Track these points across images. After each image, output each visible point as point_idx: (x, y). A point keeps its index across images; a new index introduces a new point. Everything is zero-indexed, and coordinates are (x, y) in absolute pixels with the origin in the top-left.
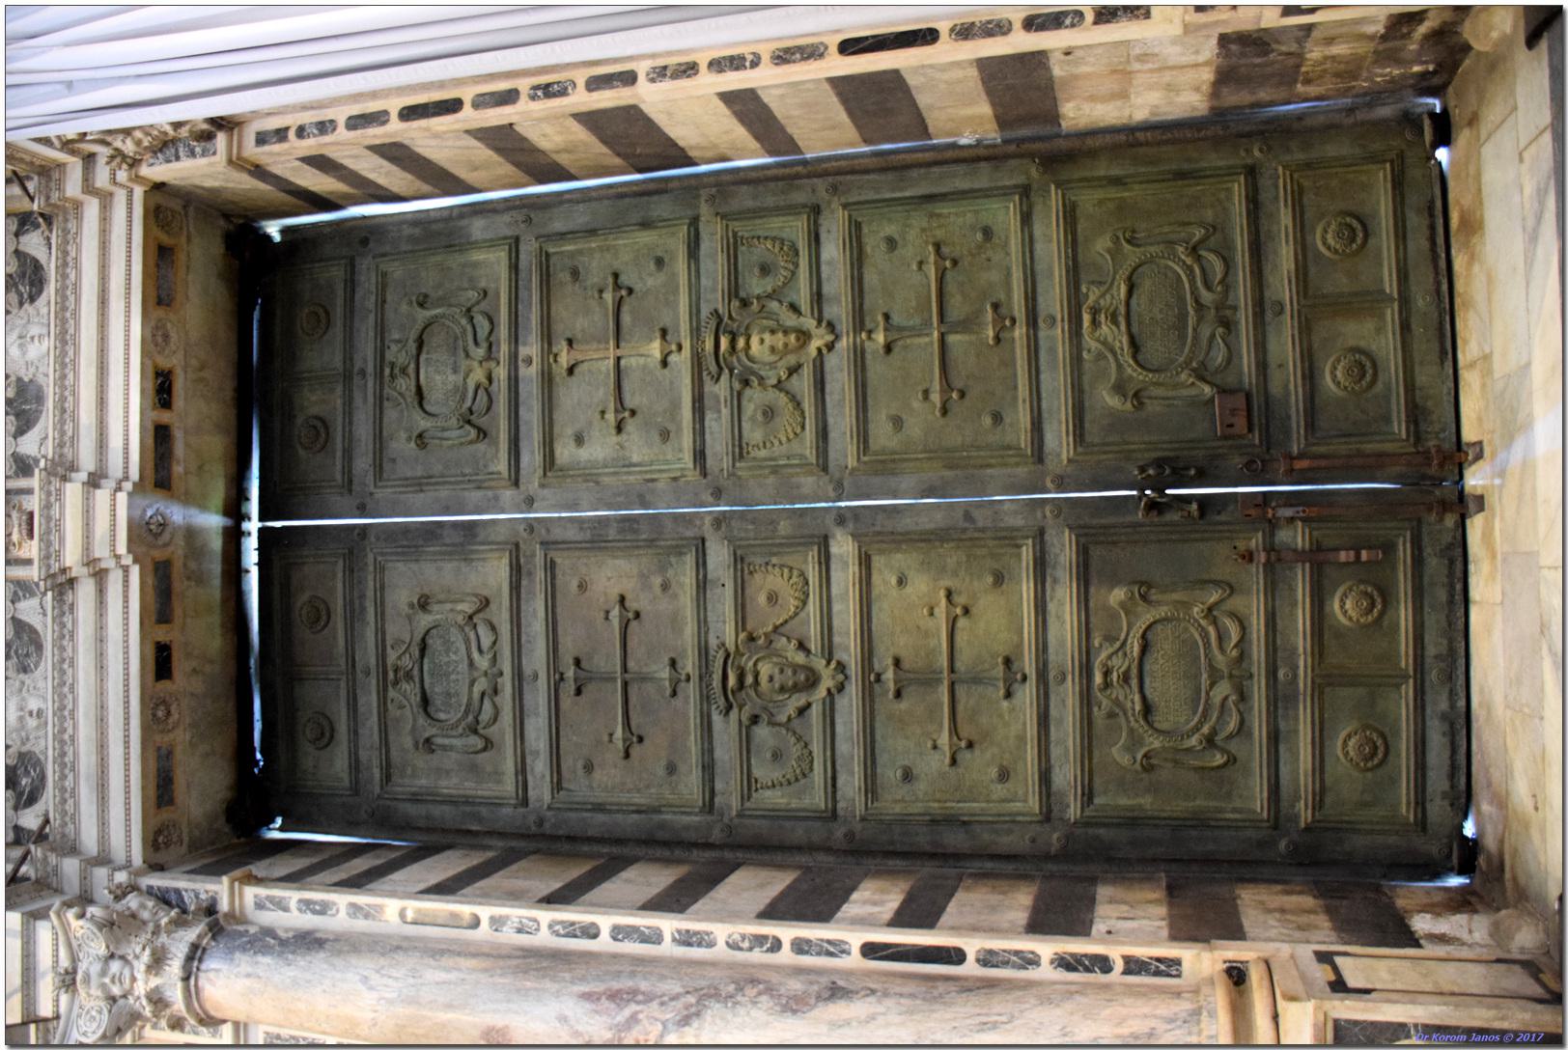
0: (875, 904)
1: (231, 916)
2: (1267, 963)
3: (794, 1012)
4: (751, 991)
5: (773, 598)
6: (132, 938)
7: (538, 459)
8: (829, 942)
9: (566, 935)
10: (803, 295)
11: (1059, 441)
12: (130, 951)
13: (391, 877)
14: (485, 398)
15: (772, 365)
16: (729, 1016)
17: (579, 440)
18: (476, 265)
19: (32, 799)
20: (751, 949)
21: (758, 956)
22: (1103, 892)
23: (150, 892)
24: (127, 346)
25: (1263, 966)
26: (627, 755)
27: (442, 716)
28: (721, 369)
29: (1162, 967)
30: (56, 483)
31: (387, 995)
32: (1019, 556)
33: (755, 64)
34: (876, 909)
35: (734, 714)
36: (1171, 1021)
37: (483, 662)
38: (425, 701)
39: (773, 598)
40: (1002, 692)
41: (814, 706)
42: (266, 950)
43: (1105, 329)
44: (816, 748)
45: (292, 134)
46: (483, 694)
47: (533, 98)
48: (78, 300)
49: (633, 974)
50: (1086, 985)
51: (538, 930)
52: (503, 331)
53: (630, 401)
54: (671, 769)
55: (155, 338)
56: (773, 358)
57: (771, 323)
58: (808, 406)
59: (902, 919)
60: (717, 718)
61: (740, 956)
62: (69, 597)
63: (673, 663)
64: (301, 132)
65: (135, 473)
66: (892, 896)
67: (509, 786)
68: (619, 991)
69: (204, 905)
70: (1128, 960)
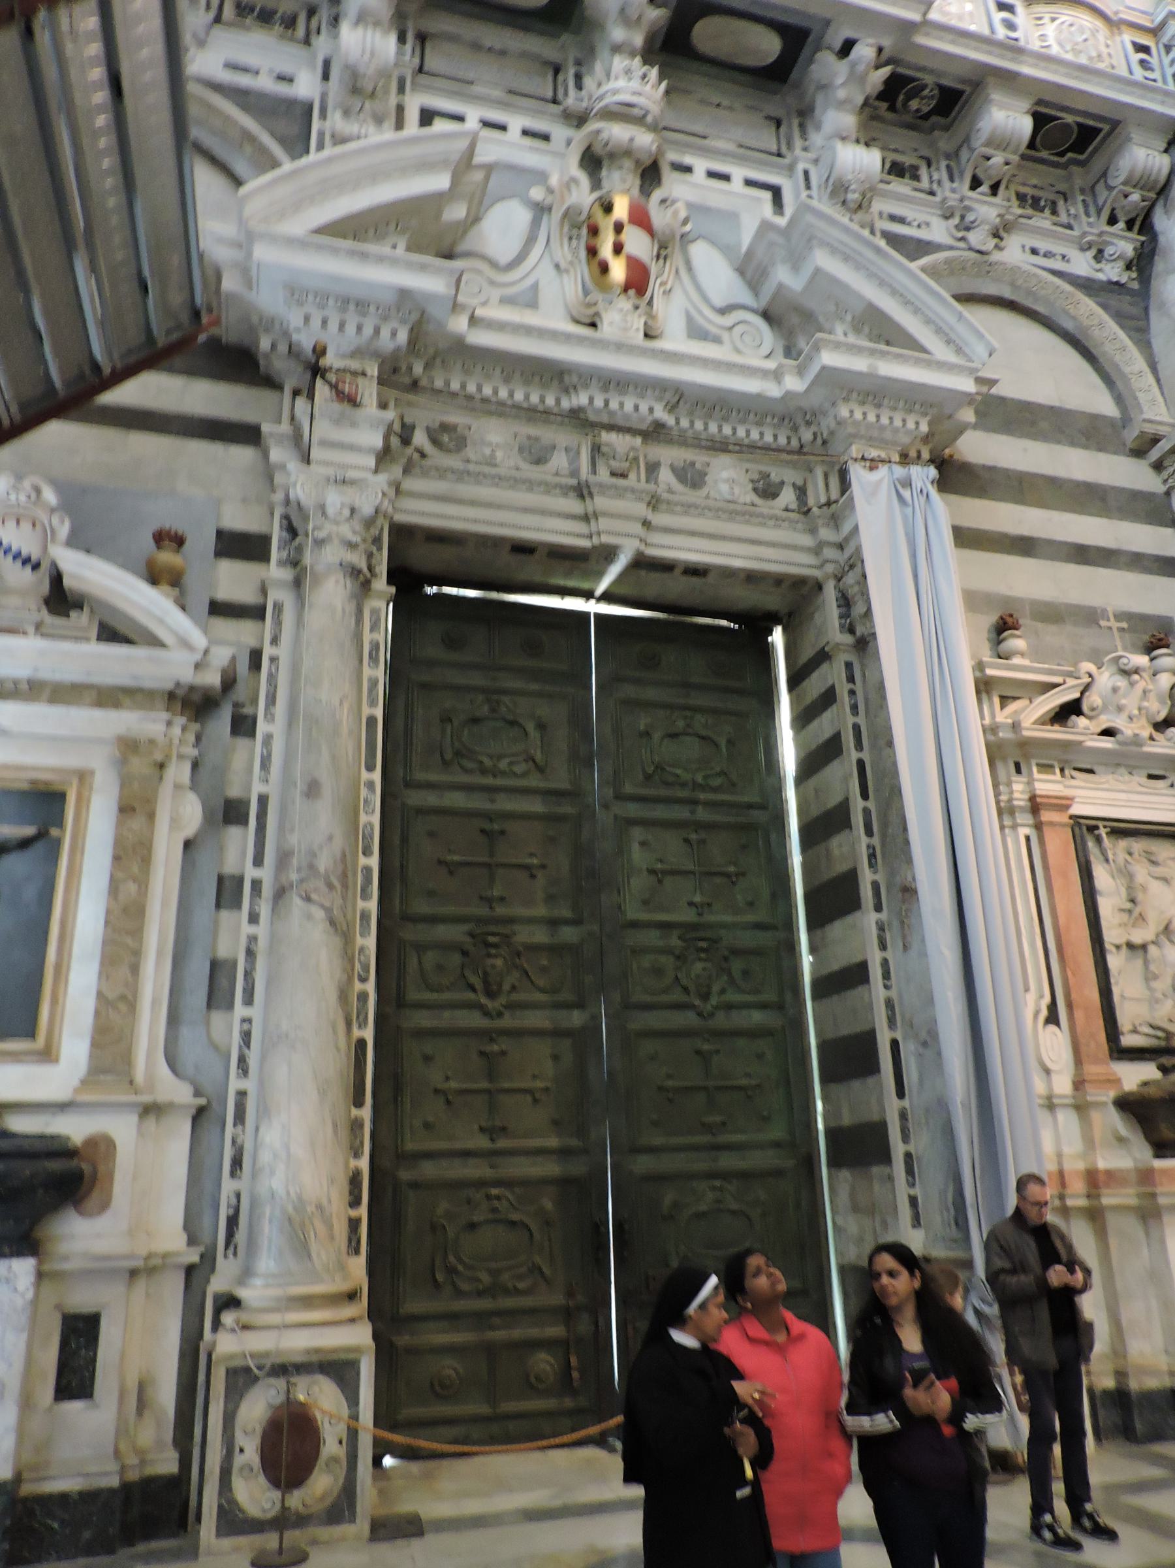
10: (733, 997)
11: (643, 1164)
19: (435, 442)
30: (648, 499)
33: (886, 987)
37: (503, 765)
38: (475, 721)
40: (483, 1124)
43: (710, 1196)
44: (447, 996)
45: (851, 686)
47: (868, 847)
52: (711, 796)
53: (668, 881)
54: (431, 894)
55: (728, 573)
56: (693, 976)
58: (665, 998)
60: (466, 927)
62: (572, 494)
63: (502, 899)
64: (852, 693)
67: (420, 776)
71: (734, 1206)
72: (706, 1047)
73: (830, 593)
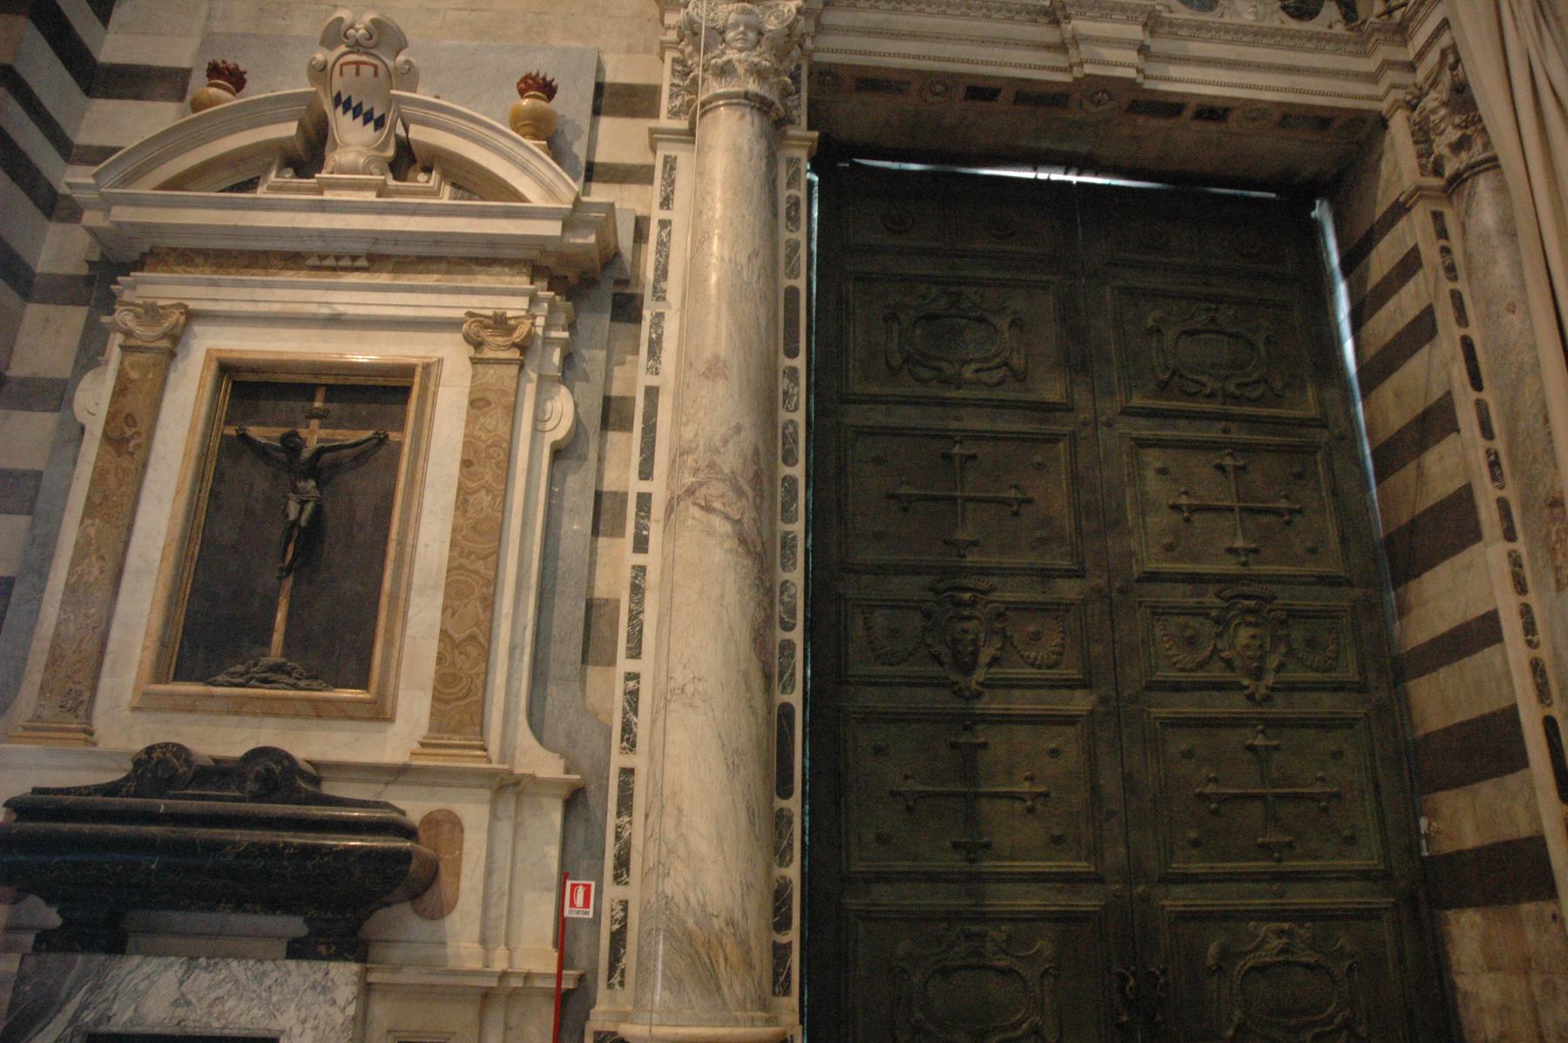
1: (784, 136)
3: (755, 640)
5: (1036, 637)
6: (774, 52)
7: (1145, 433)
8: (793, 674)
14: (1194, 390)
15: (1232, 646)
16: (748, 581)
17: (1162, 471)
18: (1303, 389)
24: (1255, 87)
26: (892, 496)
27: (918, 332)
28: (1226, 600)
29: (781, 979)
30: (1142, 19)
32: (1079, 859)
33: (1530, 643)
35: (930, 596)
39: (1036, 637)
41: (941, 669)
43: (1276, 943)
44: (904, 669)
45: (1443, 242)
46: (939, 370)
47: (1488, 452)
48: (1290, 48)
51: (787, 410)
52: (1249, 410)
53: (1197, 518)
55: (1255, 111)
57: (1268, 647)
58: (1200, 675)
60: (927, 580)
63: (975, 543)
64: (1445, 251)
65: (1149, 85)
70: (788, 947)
71: (1309, 957)
72: (1259, 741)
73: (1399, 127)
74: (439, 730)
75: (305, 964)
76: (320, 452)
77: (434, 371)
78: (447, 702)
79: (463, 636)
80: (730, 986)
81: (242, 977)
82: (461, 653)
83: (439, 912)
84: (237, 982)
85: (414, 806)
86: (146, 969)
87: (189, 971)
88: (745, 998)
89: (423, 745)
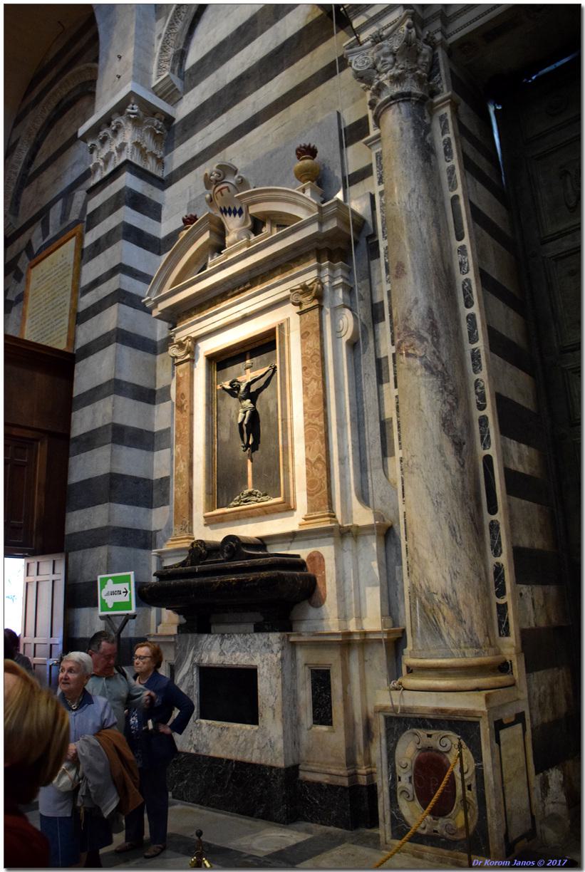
0: (520, 458)
2: (513, 685)
3: (443, 425)
4: (450, 399)
6: (406, 60)
8: (489, 436)
9: (464, 290)
12: (399, 62)
13: (478, 183)
20: (477, 394)
21: (474, 398)
22: (552, 590)
23: (434, 56)
25: (509, 682)
29: (503, 626)
31: (408, 206)
34: (516, 460)
36: (471, 631)
42: (416, 132)
49: (448, 333)
50: (488, 585)
59: (509, 475)
61: (472, 388)
66: (526, 466)
68: (436, 327)
69: (435, 89)
70: (505, 605)
74: (312, 511)
75: (260, 634)
76: (249, 385)
77: (285, 326)
78: (313, 495)
79: (315, 459)
80: (449, 634)
81: (240, 642)
82: (315, 468)
83: (319, 603)
84: (238, 644)
85: (303, 552)
86: (209, 640)
87: (222, 640)
88: (459, 640)
89: (306, 519)
